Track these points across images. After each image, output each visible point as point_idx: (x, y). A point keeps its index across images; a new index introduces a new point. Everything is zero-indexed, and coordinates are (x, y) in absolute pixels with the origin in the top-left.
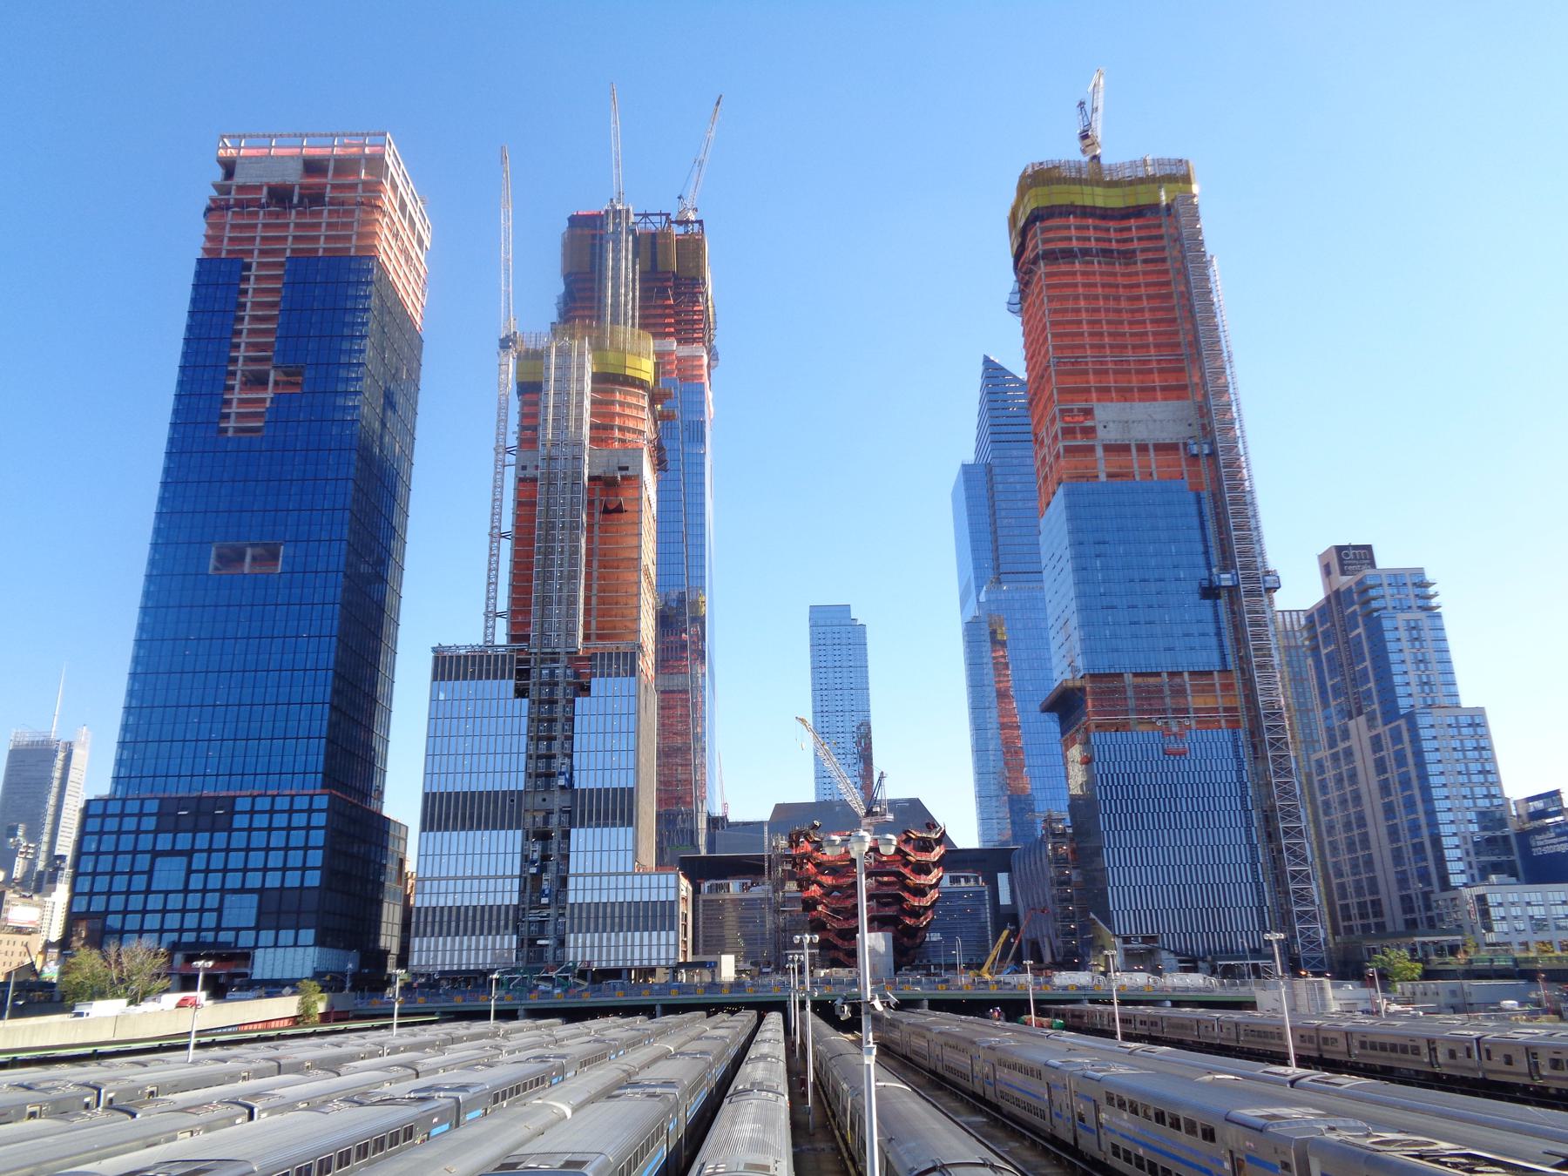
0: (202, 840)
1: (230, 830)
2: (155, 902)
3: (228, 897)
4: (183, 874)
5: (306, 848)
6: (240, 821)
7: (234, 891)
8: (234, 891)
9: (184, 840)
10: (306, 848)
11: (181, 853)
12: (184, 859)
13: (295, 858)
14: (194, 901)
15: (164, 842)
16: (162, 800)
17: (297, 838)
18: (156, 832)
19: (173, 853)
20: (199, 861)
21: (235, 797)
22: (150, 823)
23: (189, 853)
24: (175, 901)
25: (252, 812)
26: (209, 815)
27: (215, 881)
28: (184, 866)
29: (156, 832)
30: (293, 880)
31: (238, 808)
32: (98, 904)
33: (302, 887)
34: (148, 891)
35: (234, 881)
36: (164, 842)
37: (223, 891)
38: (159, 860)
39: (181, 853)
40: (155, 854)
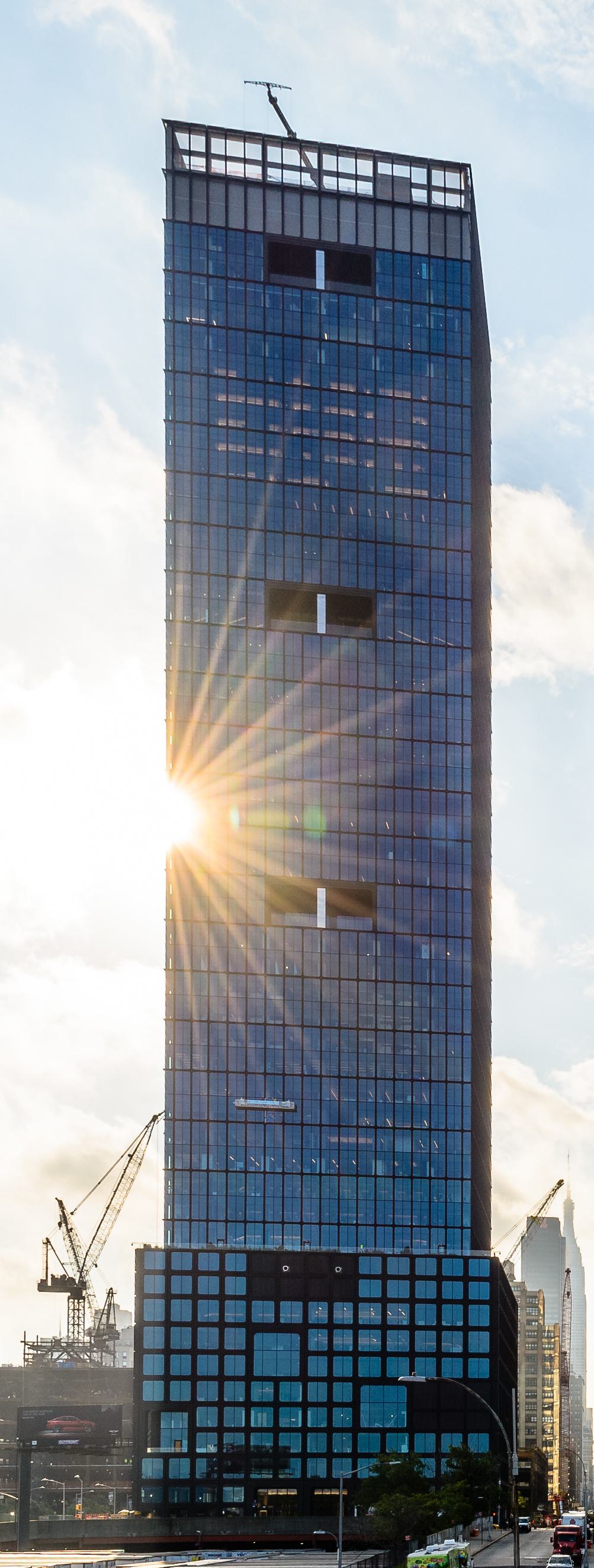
0: (319, 1312)
1: (356, 1300)
2: (262, 1391)
3: (365, 1389)
4: (297, 1356)
5: (466, 1329)
6: (367, 1288)
7: (371, 1381)
8: (371, 1381)
9: (291, 1311)
10: (466, 1329)
11: (289, 1328)
12: (297, 1338)
13: (453, 1343)
14: (317, 1392)
15: (263, 1312)
16: (250, 1254)
17: (452, 1315)
18: (249, 1298)
19: (277, 1327)
20: (317, 1340)
21: (356, 1257)
22: (237, 1286)
23: (302, 1329)
24: (293, 1392)
25: (384, 1277)
26: (327, 1277)
27: (343, 1367)
28: (297, 1346)
29: (249, 1298)
30: (452, 1369)
31: (363, 1270)
32: (181, 1392)
33: (466, 1380)
34: (249, 1378)
35: (369, 1367)
36: (263, 1312)
37: (357, 1382)
38: (257, 1337)
39: (289, 1328)
40: (252, 1328)
